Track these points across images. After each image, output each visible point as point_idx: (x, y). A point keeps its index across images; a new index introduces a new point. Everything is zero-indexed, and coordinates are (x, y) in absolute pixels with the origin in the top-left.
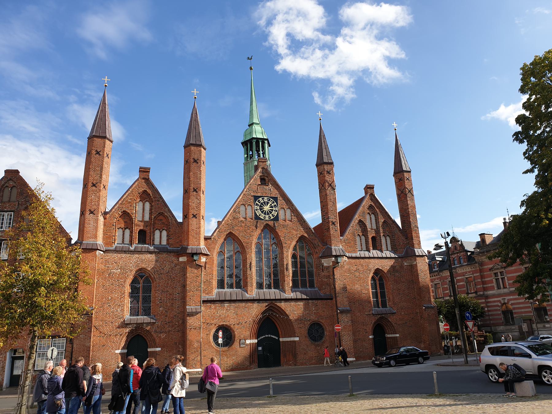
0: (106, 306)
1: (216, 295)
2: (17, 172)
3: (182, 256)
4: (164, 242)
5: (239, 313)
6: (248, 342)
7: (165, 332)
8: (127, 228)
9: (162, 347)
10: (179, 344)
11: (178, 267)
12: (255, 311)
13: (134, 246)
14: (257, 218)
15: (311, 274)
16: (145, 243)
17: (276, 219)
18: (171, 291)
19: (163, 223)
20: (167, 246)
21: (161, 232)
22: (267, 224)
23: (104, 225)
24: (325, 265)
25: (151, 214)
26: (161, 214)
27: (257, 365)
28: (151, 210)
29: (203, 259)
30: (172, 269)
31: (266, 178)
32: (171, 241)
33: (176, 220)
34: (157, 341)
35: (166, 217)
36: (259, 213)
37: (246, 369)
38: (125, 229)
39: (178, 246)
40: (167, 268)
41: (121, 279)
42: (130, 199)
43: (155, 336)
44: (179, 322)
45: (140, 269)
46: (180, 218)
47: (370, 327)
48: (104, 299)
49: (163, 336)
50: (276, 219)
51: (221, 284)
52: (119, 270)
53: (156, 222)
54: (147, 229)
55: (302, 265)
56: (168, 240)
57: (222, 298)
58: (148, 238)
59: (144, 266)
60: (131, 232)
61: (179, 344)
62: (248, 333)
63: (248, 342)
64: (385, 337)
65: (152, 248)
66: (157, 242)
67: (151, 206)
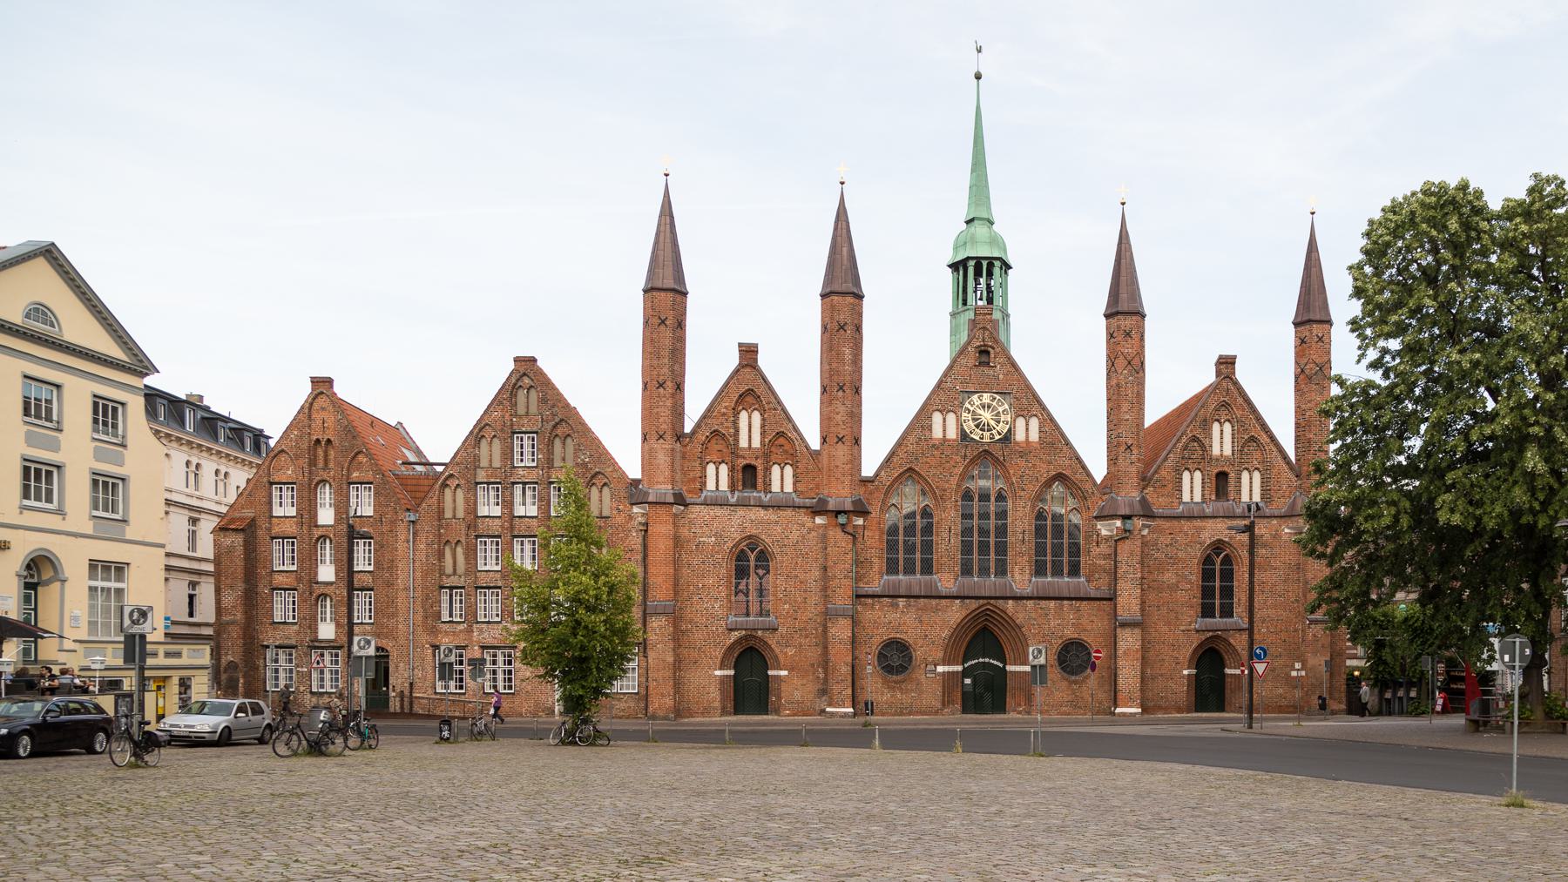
2: (533, 360)
4: (789, 488)
5: (925, 618)
6: (940, 669)
9: (791, 670)
12: (955, 613)
14: (964, 436)
15: (1075, 550)
16: (754, 486)
17: (1007, 438)
18: (802, 577)
23: (684, 458)
24: (1104, 532)
25: (763, 434)
26: (780, 434)
27: (958, 707)
28: (763, 426)
29: (860, 522)
32: (801, 487)
33: (807, 447)
34: (781, 658)
36: (969, 426)
37: (936, 713)
40: (795, 535)
43: (777, 651)
45: (750, 537)
46: (814, 443)
47: (1187, 652)
49: (791, 651)
50: (1007, 438)
51: (892, 568)
54: (759, 464)
55: (1058, 531)
58: (760, 481)
59: (754, 532)
60: (732, 470)
62: (941, 654)
63: (940, 669)
64: (1224, 675)
65: (766, 499)
66: (776, 487)
67: (764, 420)
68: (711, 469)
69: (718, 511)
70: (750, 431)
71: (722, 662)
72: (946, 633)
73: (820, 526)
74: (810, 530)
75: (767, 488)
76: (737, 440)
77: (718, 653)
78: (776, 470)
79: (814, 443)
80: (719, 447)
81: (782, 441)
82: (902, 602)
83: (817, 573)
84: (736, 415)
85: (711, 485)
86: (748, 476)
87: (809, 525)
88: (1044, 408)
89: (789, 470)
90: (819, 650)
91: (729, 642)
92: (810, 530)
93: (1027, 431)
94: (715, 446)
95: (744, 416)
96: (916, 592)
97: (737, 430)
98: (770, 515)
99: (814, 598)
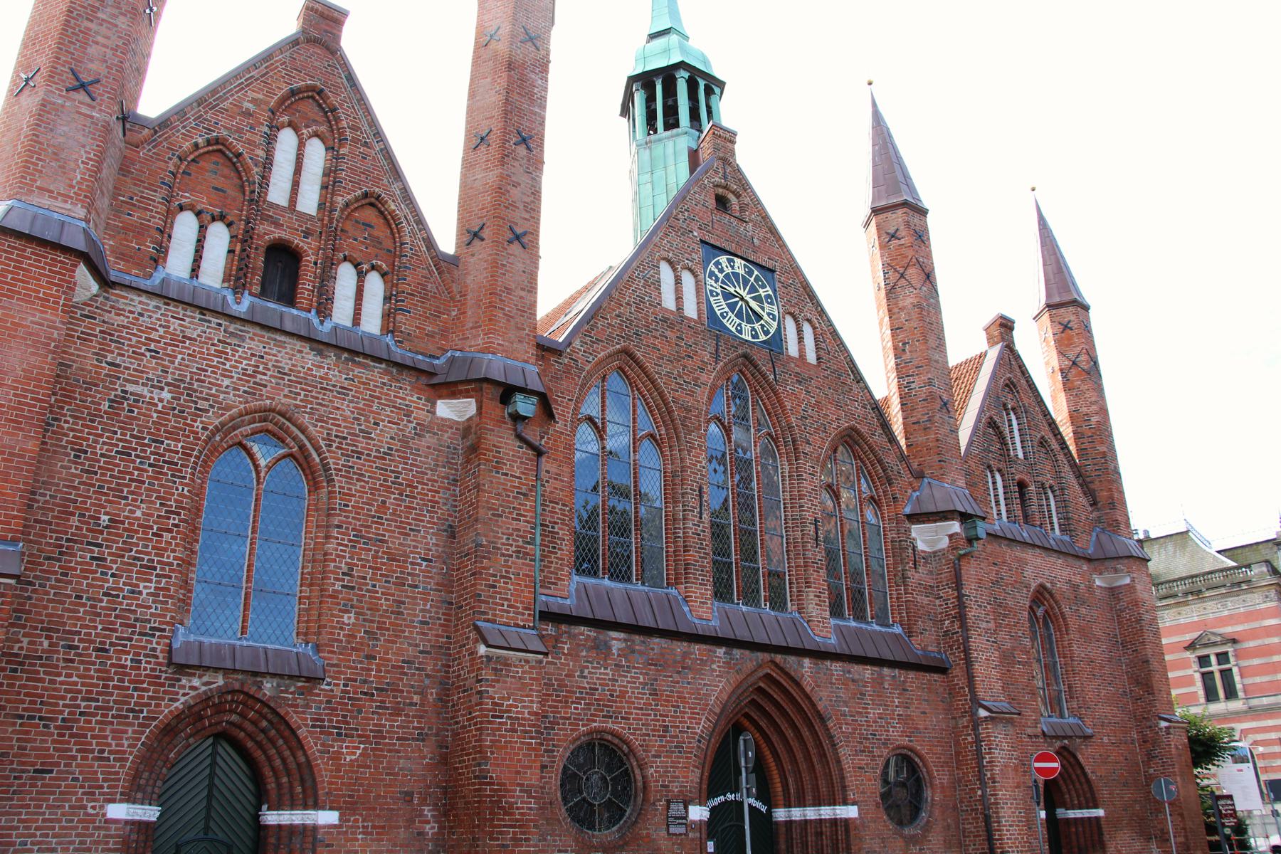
0: (82, 556)
1: (579, 597)
3: (453, 395)
4: (372, 323)
7: (364, 738)
8: (222, 218)
9: (347, 809)
10: (423, 802)
11: (429, 439)
13: (247, 301)
16: (289, 299)
19: (376, 241)
20: (388, 339)
21: (361, 276)
22: (745, 356)
23: (124, 169)
26: (372, 201)
30: (405, 442)
31: (731, 197)
33: (430, 243)
34: (324, 772)
35: (389, 220)
38: (214, 219)
39: (432, 349)
40: (384, 435)
41: (174, 435)
42: (254, 101)
43: (313, 746)
44: (423, 694)
46: (447, 241)
48: (75, 521)
49: (351, 752)
52: (166, 395)
53: (349, 226)
56: (387, 316)
57: (602, 614)
58: (307, 285)
59: (282, 401)
61: (423, 802)
66: (342, 312)
68: (185, 226)
69: (193, 326)
70: (297, 174)
71: (136, 776)
72: (702, 726)
73: (446, 424)
74: (422, 430)
75: (324, 306)
76: (265, 179)
77: (129, 743)
78: (346, 276)
79: (447, 241)
80: (220, 182)
81: (369, 215)
82: (616, 640)
83: (430, 540)
84: (275, 128)
85: (177, 264)
86: (278, 268)
87: (422, 415)
88: (822, 312)
89: (375, 285)
90: (428, 752)
91: (169, 709)
92: (422, 430)
93: (799, 343)
94: (214, 174)
95: (287, 139)
96: (647, 621)
97: (268, 164)
98: (330, 369)
99: (422, 607)
